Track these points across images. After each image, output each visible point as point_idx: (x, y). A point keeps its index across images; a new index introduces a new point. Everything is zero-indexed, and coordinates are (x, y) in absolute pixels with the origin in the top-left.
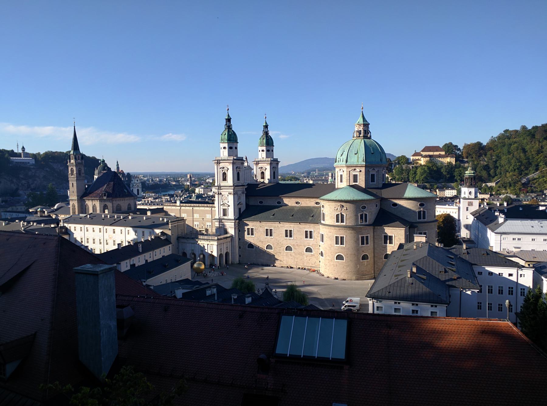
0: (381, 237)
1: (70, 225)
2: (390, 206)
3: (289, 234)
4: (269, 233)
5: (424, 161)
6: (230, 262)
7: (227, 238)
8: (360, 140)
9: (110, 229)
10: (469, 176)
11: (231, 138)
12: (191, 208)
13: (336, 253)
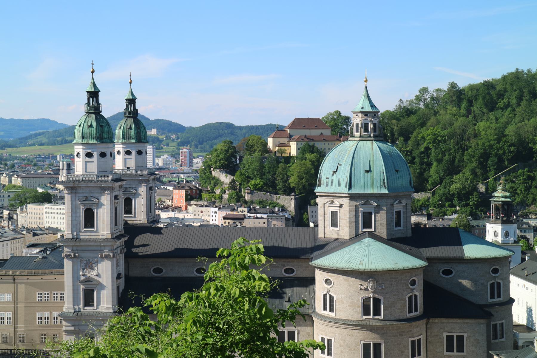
0: (440, 338)
2: (439, 273)
5: (299, 149)
10: (502, 201)
11: (104, 135)
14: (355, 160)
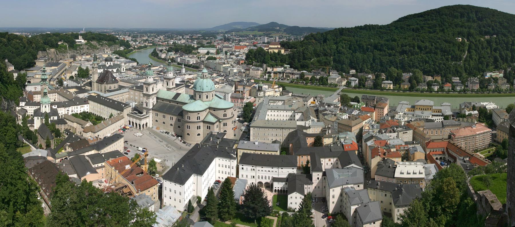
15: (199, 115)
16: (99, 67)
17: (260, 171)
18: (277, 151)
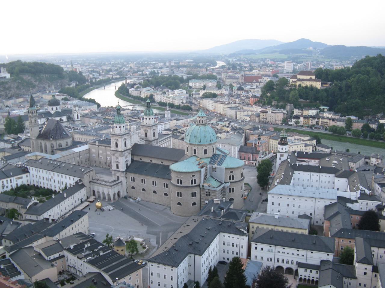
1: (29, 167)
3: (154, 183)
4: (143, 181)
6: (121, 197)
7: (119, 183)
8: (199, 127)
9: (52, 173)
12: (105, 147)
13: (178, 201)
14: (193, 133)
15: (194, 178)
16: (40, 116)
17: (281, 252)
18: (306, 229)
